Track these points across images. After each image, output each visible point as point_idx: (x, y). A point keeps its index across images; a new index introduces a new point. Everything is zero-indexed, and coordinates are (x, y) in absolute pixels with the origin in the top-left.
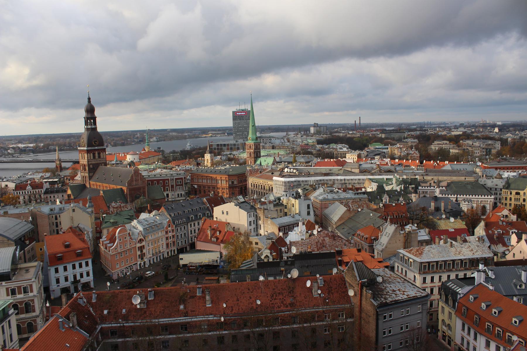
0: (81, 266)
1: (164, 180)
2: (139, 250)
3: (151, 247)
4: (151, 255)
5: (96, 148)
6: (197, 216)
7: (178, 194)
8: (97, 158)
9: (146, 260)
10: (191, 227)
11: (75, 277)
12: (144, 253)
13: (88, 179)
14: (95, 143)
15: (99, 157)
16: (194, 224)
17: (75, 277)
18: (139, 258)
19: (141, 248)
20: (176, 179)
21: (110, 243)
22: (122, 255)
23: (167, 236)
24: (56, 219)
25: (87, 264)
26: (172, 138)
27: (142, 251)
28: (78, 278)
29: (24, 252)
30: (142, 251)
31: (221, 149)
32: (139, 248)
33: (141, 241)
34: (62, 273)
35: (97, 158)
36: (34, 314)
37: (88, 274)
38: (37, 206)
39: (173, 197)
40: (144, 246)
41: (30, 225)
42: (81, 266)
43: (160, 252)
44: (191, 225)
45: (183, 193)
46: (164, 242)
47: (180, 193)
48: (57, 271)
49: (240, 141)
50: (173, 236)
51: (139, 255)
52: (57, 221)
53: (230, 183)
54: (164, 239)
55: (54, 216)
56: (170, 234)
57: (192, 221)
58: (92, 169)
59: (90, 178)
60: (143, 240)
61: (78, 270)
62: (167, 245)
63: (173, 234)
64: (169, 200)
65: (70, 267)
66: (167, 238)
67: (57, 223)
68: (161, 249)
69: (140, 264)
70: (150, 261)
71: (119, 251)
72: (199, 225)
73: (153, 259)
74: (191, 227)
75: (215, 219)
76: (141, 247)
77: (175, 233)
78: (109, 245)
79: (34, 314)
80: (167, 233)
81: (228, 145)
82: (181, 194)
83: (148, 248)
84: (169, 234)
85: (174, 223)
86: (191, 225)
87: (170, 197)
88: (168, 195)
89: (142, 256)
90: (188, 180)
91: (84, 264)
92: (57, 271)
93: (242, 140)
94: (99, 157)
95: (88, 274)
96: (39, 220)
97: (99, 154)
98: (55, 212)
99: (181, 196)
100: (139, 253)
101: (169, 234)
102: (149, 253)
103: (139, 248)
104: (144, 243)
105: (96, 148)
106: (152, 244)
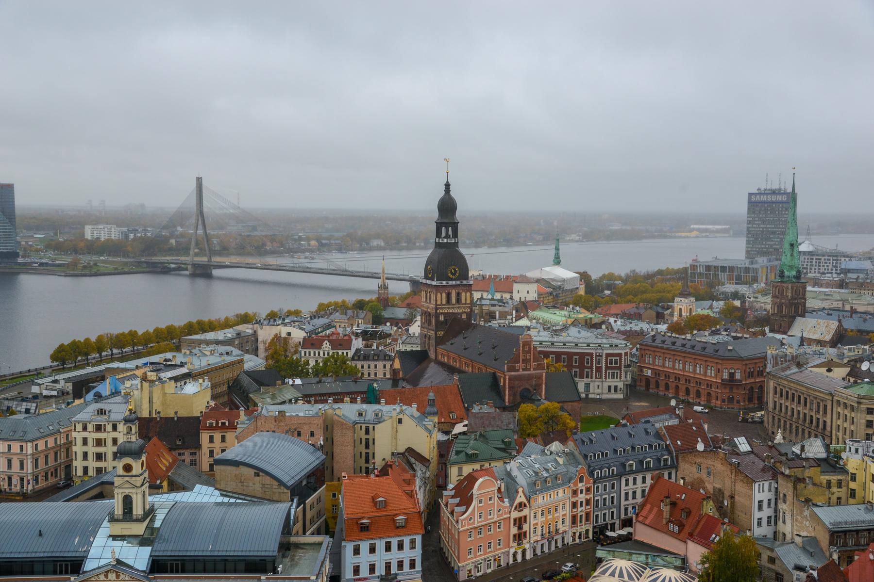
0: (401, 547)
1: (582, 355)
2: (515, 524)
3: (540, 519)
4: (539, 538)
5: (454, 283)
6: (641, 462)
7: (610, 387)
8: (454, 301)
9: (527, 546)
10: (627, 485)
11: (388, 566)
12: (525, 533)
13: (433, 342)
14: (451, 273)
15: (458, 301)
16: (635, 479)
17: (388, 566)
18: (514, 540)
19: (520, 522)
20: (608, 355)
21: (458, 505)
22: (480, 533)
23: (575, 500)
24: (367, 432)
26: (612, 236)
27: (520, 528)
28: (394, 569)
29: (304, 508)
30: (520, 528)
32: (515, 520)
33: (521, 506)
34: (364, 559)
35: (454, 301)
37: (412, 564)
38: (336, 406)
39: (600, 391)
40: (525, 517)
41: (319, 453)
42: (401, 547)
43: (557, 531)
44: (627, 481)
45: (620, 385)
47: (613, 384)
48: (357, 551)
50: (588, 502)
51: (514, 536)
52: (367, 437)
53: (726, 376)
54: (568, 506)
55: (364, 426)
57: (631, 472)
58: (442, 322)
59: (440, 341)
60: (525, 506)
61: (394, 556)
62: (574, 518)
63: (588, 497)
64: (590, 396)
65: (380, 545)
66: (574, 505)
67: (367, 440)
68: (560, 525)
69: (515, 555)
70: (534, 550)
71: (476, 525)
72: (644, 482)
73: (542, 545)
74: (627, 485)
76: (520, 518)
77: (591, 496)
78: (457, 509)
80: (575, 493)
82: (616, 387)
83: (533, 522)
84: (580, 496)
85: (591, 474)
86: (627, 481)
87: (591, 391)
88: (587, 386)
89: (520, 537)
90: (632, 356)
91: (407, 544)
92: (357, 551)
94: (458, 301)
95: (412, 564)
96: (337, 432)
97: (458, 294)
98: (367, 419)
99: (616, 390)
100: (514, 530)
101: (580, 496)
102: (535, 532)
103: (515, 520)
104: (526, 512)
105: (454, 283)
106: (542, 514)
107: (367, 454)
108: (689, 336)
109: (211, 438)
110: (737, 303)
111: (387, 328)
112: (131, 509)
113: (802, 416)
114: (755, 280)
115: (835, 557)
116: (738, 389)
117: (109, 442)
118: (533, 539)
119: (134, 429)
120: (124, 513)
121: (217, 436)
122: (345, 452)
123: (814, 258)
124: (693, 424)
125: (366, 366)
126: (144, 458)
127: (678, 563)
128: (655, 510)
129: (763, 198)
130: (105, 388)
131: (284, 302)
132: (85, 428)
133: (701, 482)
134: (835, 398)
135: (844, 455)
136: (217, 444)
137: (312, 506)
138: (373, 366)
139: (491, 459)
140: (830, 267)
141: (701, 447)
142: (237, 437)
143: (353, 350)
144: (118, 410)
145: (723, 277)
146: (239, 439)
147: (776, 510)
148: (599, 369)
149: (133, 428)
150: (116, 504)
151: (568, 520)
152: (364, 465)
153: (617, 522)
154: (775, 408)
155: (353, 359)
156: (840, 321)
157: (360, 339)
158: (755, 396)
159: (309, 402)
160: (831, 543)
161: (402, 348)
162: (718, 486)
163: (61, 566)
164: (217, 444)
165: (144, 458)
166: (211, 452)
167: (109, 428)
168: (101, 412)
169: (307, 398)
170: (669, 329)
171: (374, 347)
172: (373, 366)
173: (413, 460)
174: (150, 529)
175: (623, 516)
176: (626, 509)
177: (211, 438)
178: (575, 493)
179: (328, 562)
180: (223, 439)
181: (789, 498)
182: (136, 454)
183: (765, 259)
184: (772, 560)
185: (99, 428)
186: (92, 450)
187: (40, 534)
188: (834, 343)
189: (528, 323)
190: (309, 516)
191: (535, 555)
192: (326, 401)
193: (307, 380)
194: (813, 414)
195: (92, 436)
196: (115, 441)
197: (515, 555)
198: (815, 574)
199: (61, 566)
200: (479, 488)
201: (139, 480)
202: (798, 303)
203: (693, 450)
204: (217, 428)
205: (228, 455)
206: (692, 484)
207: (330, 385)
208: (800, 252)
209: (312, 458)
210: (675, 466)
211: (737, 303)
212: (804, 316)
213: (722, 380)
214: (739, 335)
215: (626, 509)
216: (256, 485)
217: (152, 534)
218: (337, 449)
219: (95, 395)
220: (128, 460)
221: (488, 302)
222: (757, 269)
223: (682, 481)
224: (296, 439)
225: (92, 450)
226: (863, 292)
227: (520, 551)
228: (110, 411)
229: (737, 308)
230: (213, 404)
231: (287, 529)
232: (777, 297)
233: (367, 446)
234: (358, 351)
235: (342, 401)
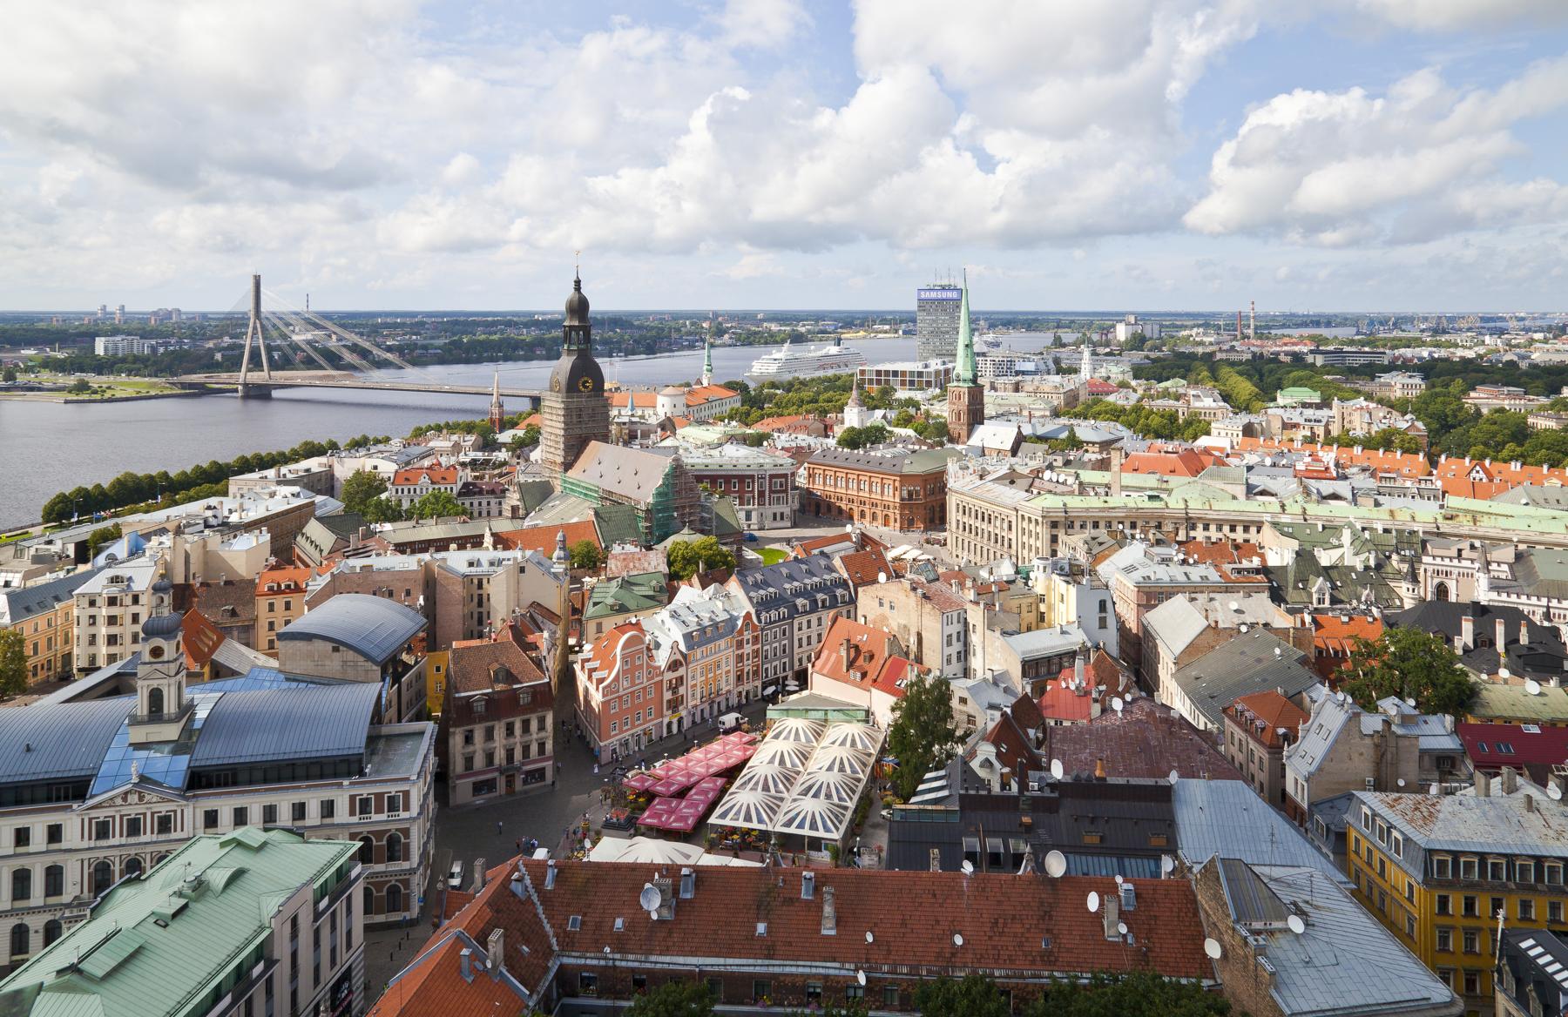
9: (684, 713)
11: (510, 754)
17: (510, 754)
24: (480, 586)
25: (542, 728)
31: (887, 382)
36: (406, 865)
46: (732, 667)
48: (469, 739)
49: (935, 365)
53: (905, 494)
54: (732, 661)
56: (748, 649)
66: (740, 658)
69: (669, 725)
75: (862, 621)
79: (406, 865)
81: (904, 373)
83: (691, 683)
92: (469, 739)
93: (939, 361)
100: (668, 696)
104: (681, 671)
107: (480, 614)
108: (861, 452)
109: (271, 606)
111: (502, 455)
112: (160, 708)
115: (1028, 689)
117: (129, 619)
118: (691, 704)
119: (167, 599)
120: (150, 711)
121: (279, 602)
122: (453, 612)
124: (872, 553)
125: (476, 503)
126: (180, 637)
127: (862, 715)
128: (834, 656)
130: (120, 549)
131: (369, 425)
132: (92, 603)
133: (884, 618)
135: (1032, 575)
136: (280, 614)
137: (410, 685)
138: (484, 503)
139: (640, 609)
141: (882, 577)
142: (308, 603)
143: (460, 484)
144: (143, 574)
146: (312, 604)
147: (966, 644)
148: (762, 494)
149: (166, 598)
150: (138, 703)
151: (732, 678)
152: (476, 628)
153: (790, 674)
155: (460, 494)
157: (468, 471)
159: (403, 552)
160: (1024, 675)
161: (522, 479)
162: (903, 622)
163: (58, 790)
164: (280, 614)
165: (180, 637)
166: (271, 624)
167: (128, 600)
168: (115, 580)
169: (401, 548)
170: (839, 443)
171: (487, 479)
172: (484, 503)
173: (539, 619)
174: (188, 731)
175: (796, 667)
176: (800, 660)
177: (271, 606)
178: (740, 645)
179: (431, 756)
180: (288, 606)
181: (979, 628)
182: (167, 633)
184: (963, 701)
185: (112, 601)
186: (103, 630)
187: (28, 749)
189: (676, 443)
190: (404, 699)
191: (694, 722)
192: (426, 550)
193: (399, 525)
195: (104, 611)
196: (135, 618)
197: (669, 725)
198: (1008, 711)
199: (58, 790)
200: (624, 648)
201: (173, 667)
203: (875, 581)
204: (279, 592)
205: (297, 625)
206: (875, 622)
207: (432, 530)
209: (411, 624)
210: (853, 601)
215: (800, 660)
216: (333, 664)
217: (190, 738)
218: (440, 610)
219: (108, 557)
220: (158, 642)
221: (626, 420)
223: (862, 621)
224: (386, 601)
225: (103, 630)
227: (675, 721)
228: (130, 579)
230: (273, 560)
231: (377, 717)
233: (480, 604)
234: (466, 485)
235: (446, 549)
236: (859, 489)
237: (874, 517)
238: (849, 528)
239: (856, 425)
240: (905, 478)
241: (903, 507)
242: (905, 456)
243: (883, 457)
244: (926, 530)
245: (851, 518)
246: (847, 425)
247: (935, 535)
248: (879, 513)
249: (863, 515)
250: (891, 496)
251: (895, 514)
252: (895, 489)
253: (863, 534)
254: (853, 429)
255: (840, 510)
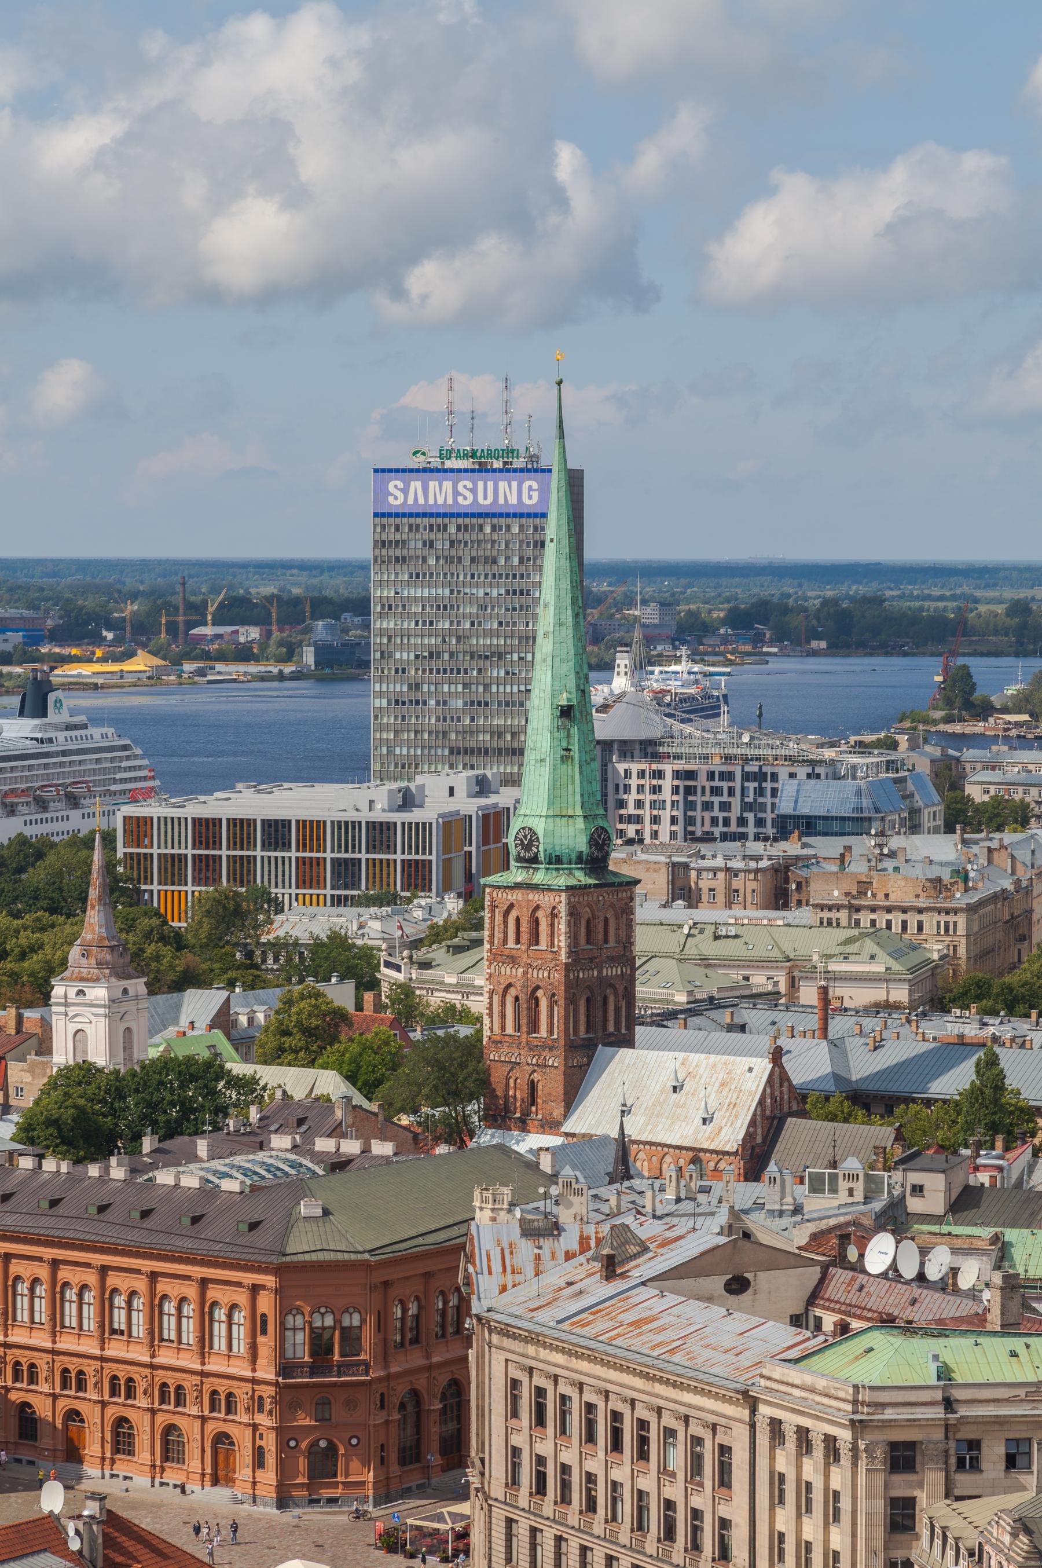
110: (340, 993)
113: (627, 1508)
114: (417, 877)
116: (351, 1404)
123: (668, 768)
129: (440, 494)
134: (765, 1411)
140: (734, 814)
145: (274, 869)
154: (513, 1482)
156: (777, 1056)
158: (434, 1431)
170: (28, 1134)
183: (461, 779)
188: (755, 1157)
194: (674, 1491)
202: (604, 983)
208: (606, 745)
211: (340, 993)
212: (629, 1042)
213: (286, 1368)
214: (351, 1147)
222: (423, 828)
226: (865, 918)
229: (340, 1016)
232: (512, 960)
236: (107, 1331)
237: (170, 1447)
238: (52, 1499)
239: (99, 1056)
240: (298, 1278)
241: (288, 1398)
242: (298, 1187)
243: (209, 1192)
244: (385, 1495)
245: (73, 1454)
246: (61, 1056)
247: (413, 1515)
248: (190, 1429)
249: (122, 1439)
250: (240, 1356)
251: (252, 1429)
252: (258, 1325)
253: (112, 1520)
254: (83, 1073)
255: (27, 1423)
